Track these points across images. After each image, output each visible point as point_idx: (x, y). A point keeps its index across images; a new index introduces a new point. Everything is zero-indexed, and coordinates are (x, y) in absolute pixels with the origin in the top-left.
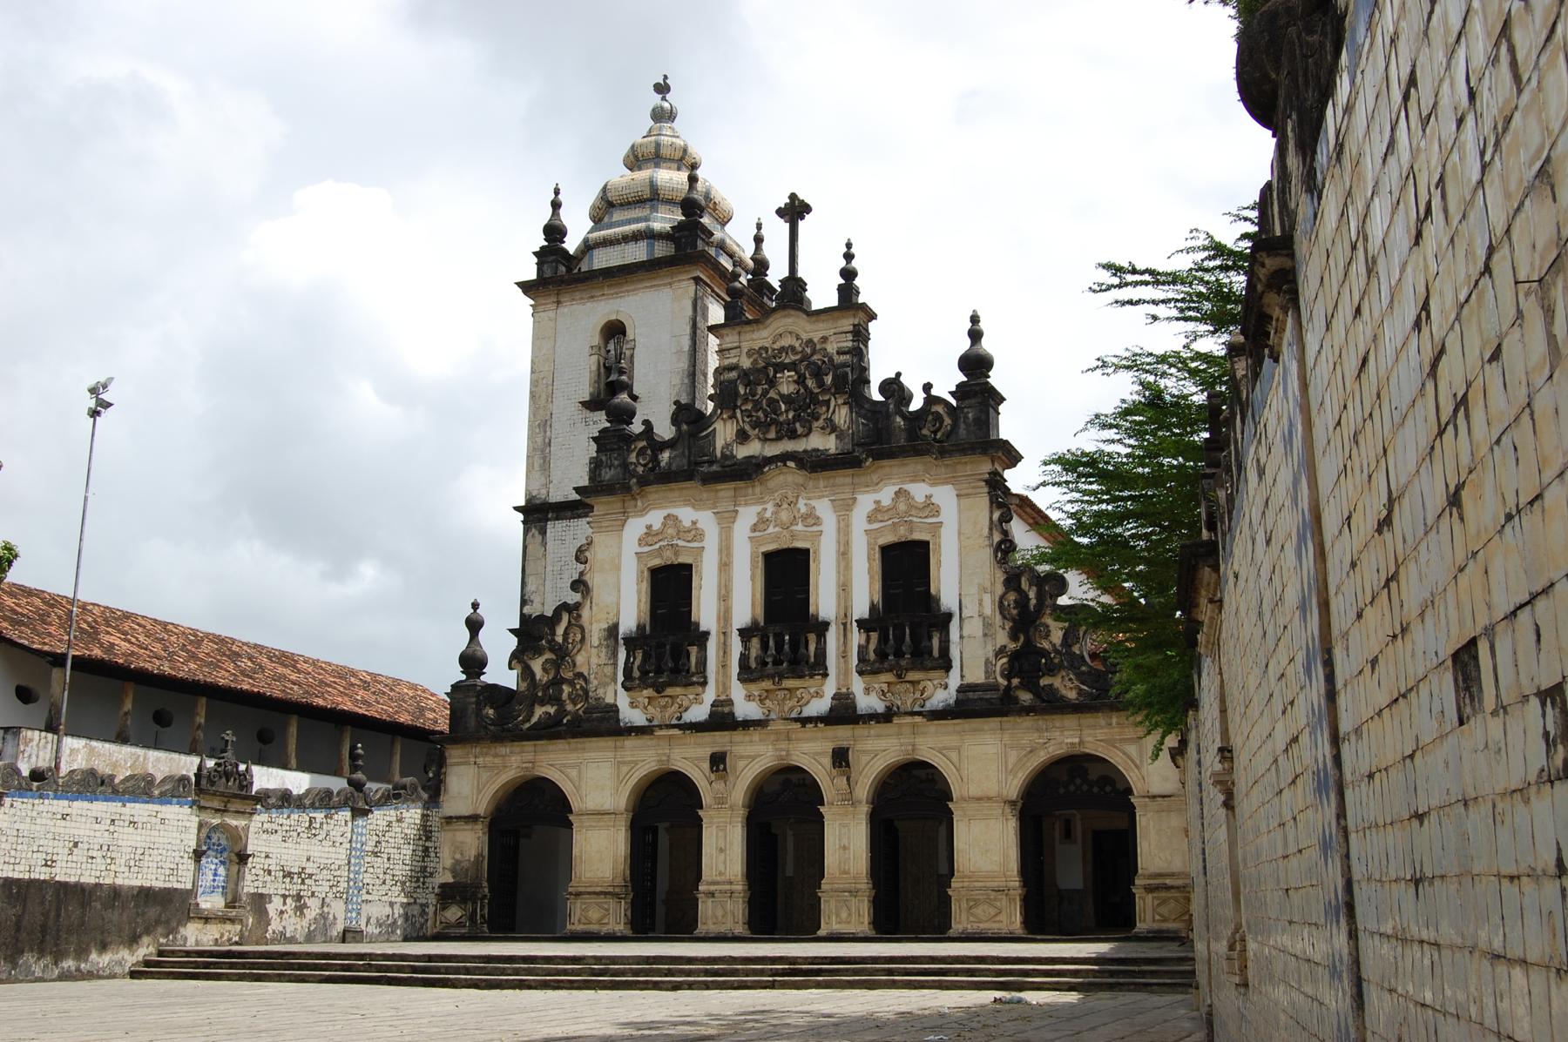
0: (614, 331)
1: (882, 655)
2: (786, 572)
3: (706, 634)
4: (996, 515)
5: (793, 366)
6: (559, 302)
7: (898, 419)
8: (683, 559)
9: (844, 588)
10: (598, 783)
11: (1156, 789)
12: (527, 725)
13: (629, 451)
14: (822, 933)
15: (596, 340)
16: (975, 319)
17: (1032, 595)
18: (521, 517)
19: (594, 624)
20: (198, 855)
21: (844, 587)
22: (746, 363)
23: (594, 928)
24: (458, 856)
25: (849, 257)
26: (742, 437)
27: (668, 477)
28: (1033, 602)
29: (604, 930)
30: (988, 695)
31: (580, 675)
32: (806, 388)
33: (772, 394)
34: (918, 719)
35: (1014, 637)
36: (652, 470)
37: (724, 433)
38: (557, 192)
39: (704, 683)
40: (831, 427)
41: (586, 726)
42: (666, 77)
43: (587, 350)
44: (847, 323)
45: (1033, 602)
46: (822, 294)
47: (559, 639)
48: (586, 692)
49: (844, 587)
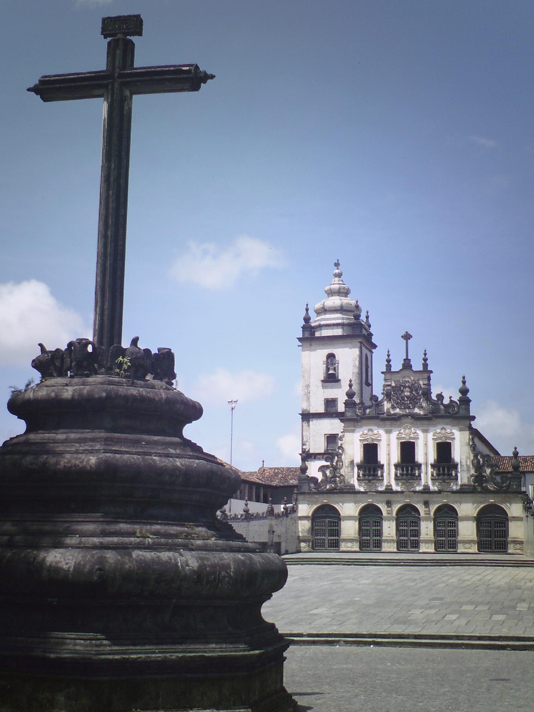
0: (331, 356)
1: (438, 475)
2: (408, 449)
3: (383, 465)
4: (471, 437)
5: (409, 387)
6: (311, 345)
7: (442, 407)
8: (375, 442)
9: (426, 454)
10: (349, 509)
11: (515, 514)
12: (325, 489)
13: (356, 408)
14: (421, 551)
15: (325, 360)
16: (464, 378)
17: (481, 460)
18: (301, 416)
19: (346, 459)
20: (269, 531)
21: (426, 453)
22: (393, 384)
23: (349, 549)
24: (303, 528)
25: (425, 354)
26: (393, 408)
27: (370, 418)
28: (481, 462)
29: (353, 550)
30: (468, 487)
31: (342, 475)
32: (413, 394)
33: (402, 395)
34: (449, 493)
35: (475, 472)
36: (364, 414)
37: (387, 406)
38: (307, 305)
39: (383, 480)
40: (421, 407)
41: (345, 490)
42: (338, 260)
43: (322, 363)
44: (426, 375)
45: (481, 462)
46: (417, 366)
47: (334, 464)
48: (344, 480)
49: (426, 453)
